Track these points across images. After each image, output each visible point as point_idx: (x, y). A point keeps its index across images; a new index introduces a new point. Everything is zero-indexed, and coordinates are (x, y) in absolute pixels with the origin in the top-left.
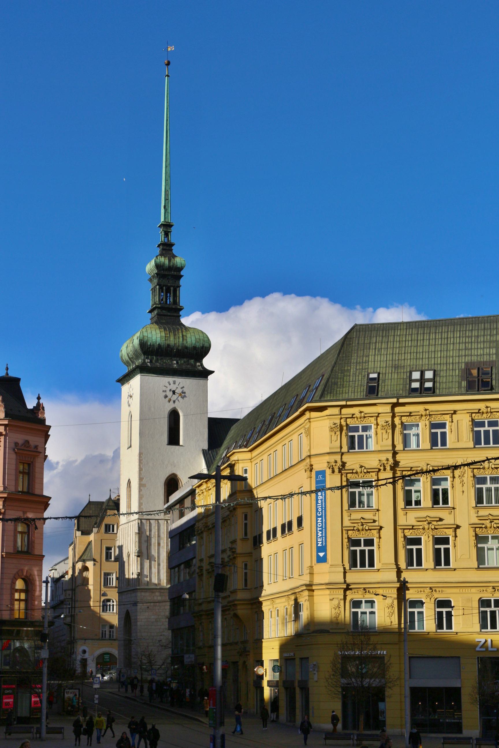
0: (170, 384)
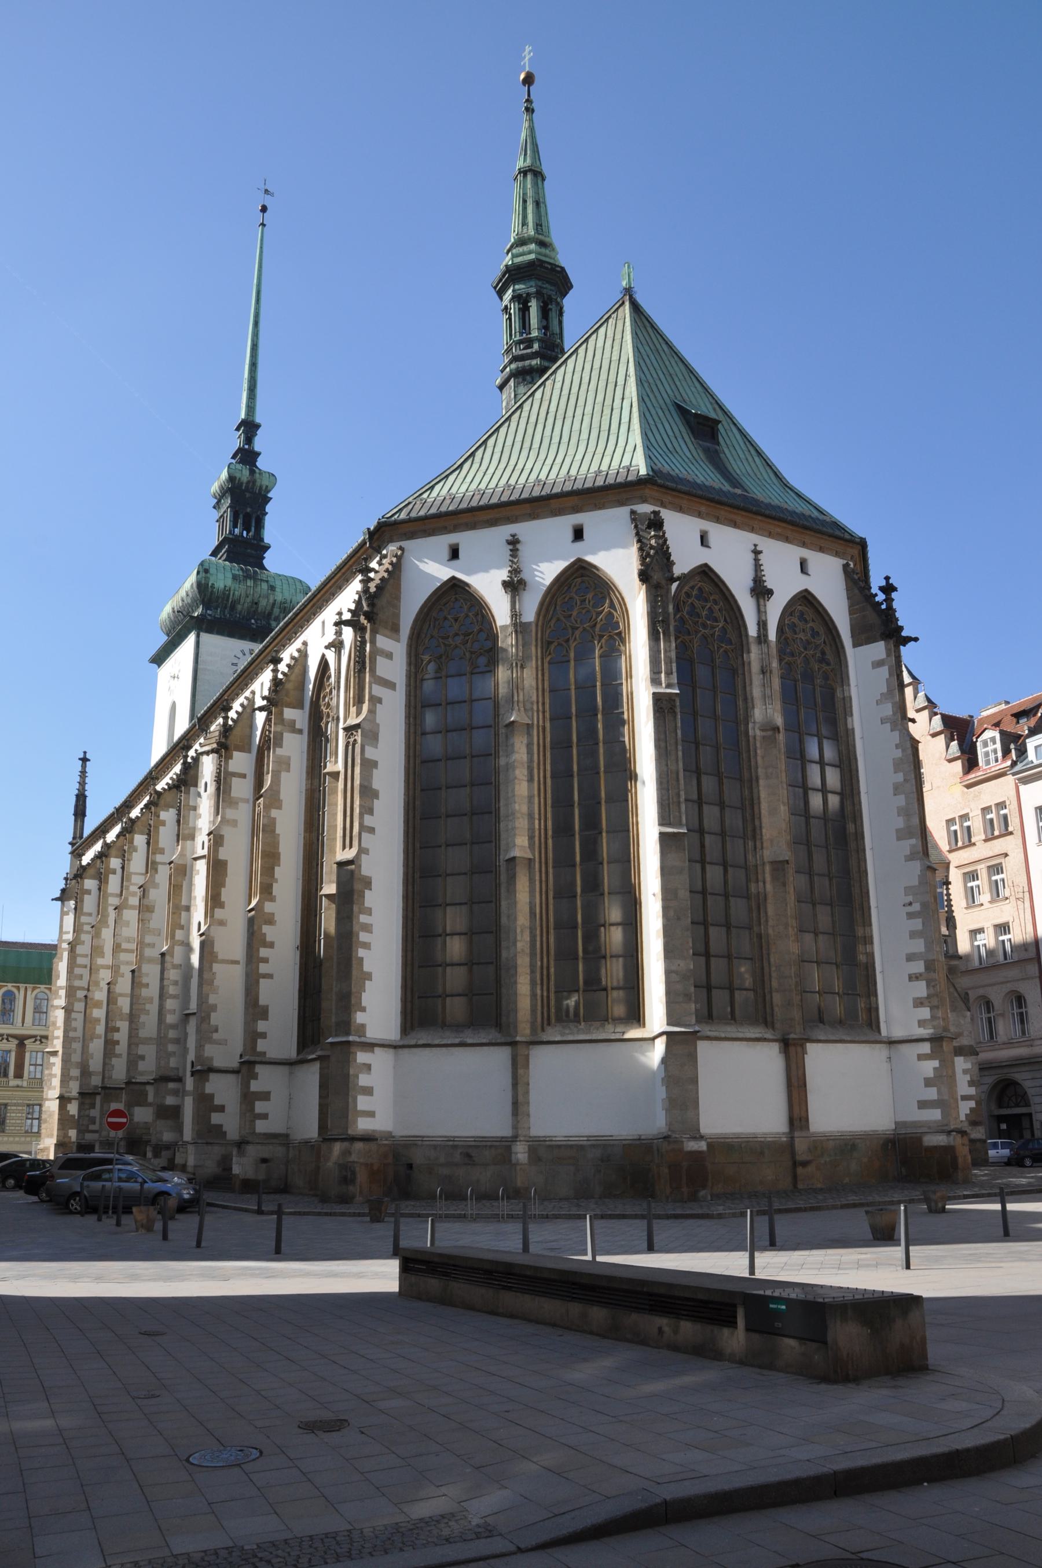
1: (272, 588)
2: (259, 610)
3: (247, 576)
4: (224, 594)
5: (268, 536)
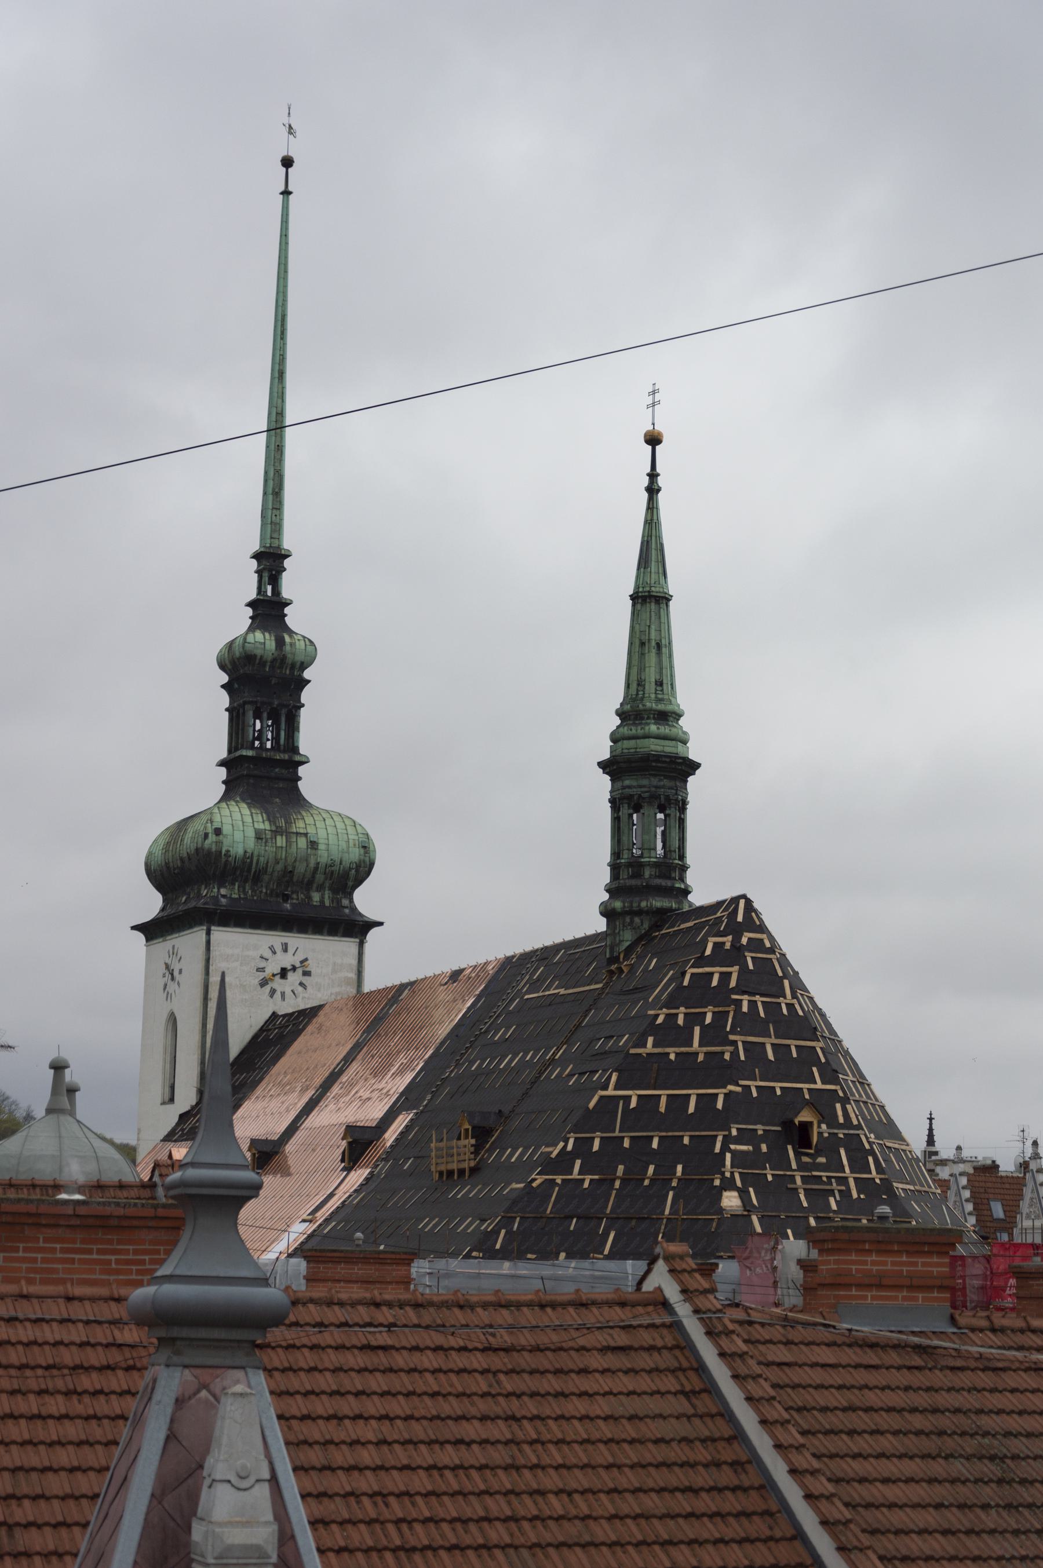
0: (274, 953)
1: (313, 845)
2: (295, 879)
3: (277, 832)
4: (244, 862)
5: (306, 741)
